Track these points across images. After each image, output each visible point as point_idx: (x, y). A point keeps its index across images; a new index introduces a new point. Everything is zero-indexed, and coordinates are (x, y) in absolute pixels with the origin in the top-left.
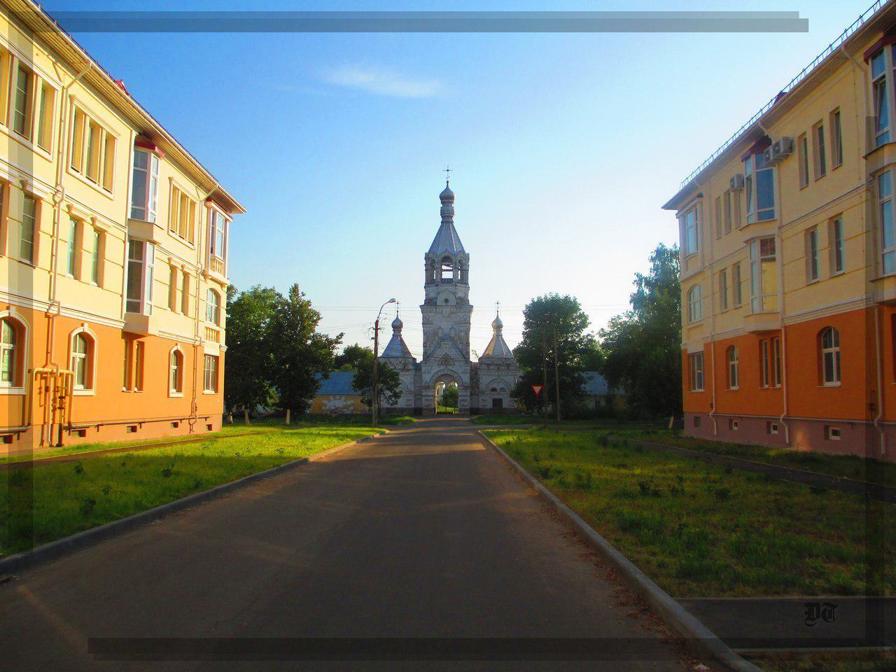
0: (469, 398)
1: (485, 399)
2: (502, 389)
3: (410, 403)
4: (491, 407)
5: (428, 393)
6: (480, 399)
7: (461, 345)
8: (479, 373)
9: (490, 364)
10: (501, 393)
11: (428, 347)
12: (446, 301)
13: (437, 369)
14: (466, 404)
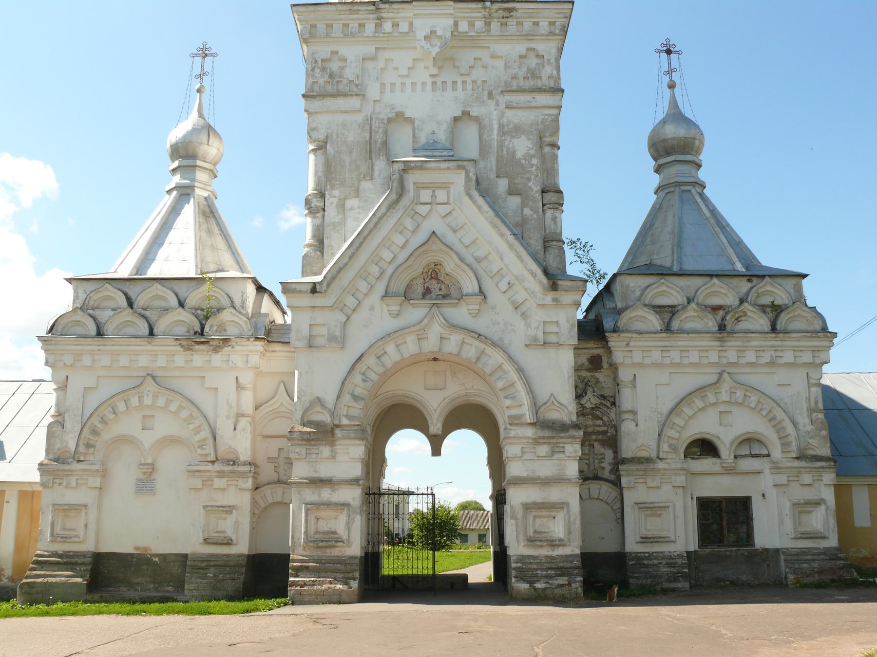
0: (571, 495)
1: (653, 497)
3: (227, 526)
4: (693, 545)
5: (325, 470)
7: (515, 201)
8: (619, 356)
9: (673, 310)
11: (331, 212)
13: (390, 324)
14: (557, 528)
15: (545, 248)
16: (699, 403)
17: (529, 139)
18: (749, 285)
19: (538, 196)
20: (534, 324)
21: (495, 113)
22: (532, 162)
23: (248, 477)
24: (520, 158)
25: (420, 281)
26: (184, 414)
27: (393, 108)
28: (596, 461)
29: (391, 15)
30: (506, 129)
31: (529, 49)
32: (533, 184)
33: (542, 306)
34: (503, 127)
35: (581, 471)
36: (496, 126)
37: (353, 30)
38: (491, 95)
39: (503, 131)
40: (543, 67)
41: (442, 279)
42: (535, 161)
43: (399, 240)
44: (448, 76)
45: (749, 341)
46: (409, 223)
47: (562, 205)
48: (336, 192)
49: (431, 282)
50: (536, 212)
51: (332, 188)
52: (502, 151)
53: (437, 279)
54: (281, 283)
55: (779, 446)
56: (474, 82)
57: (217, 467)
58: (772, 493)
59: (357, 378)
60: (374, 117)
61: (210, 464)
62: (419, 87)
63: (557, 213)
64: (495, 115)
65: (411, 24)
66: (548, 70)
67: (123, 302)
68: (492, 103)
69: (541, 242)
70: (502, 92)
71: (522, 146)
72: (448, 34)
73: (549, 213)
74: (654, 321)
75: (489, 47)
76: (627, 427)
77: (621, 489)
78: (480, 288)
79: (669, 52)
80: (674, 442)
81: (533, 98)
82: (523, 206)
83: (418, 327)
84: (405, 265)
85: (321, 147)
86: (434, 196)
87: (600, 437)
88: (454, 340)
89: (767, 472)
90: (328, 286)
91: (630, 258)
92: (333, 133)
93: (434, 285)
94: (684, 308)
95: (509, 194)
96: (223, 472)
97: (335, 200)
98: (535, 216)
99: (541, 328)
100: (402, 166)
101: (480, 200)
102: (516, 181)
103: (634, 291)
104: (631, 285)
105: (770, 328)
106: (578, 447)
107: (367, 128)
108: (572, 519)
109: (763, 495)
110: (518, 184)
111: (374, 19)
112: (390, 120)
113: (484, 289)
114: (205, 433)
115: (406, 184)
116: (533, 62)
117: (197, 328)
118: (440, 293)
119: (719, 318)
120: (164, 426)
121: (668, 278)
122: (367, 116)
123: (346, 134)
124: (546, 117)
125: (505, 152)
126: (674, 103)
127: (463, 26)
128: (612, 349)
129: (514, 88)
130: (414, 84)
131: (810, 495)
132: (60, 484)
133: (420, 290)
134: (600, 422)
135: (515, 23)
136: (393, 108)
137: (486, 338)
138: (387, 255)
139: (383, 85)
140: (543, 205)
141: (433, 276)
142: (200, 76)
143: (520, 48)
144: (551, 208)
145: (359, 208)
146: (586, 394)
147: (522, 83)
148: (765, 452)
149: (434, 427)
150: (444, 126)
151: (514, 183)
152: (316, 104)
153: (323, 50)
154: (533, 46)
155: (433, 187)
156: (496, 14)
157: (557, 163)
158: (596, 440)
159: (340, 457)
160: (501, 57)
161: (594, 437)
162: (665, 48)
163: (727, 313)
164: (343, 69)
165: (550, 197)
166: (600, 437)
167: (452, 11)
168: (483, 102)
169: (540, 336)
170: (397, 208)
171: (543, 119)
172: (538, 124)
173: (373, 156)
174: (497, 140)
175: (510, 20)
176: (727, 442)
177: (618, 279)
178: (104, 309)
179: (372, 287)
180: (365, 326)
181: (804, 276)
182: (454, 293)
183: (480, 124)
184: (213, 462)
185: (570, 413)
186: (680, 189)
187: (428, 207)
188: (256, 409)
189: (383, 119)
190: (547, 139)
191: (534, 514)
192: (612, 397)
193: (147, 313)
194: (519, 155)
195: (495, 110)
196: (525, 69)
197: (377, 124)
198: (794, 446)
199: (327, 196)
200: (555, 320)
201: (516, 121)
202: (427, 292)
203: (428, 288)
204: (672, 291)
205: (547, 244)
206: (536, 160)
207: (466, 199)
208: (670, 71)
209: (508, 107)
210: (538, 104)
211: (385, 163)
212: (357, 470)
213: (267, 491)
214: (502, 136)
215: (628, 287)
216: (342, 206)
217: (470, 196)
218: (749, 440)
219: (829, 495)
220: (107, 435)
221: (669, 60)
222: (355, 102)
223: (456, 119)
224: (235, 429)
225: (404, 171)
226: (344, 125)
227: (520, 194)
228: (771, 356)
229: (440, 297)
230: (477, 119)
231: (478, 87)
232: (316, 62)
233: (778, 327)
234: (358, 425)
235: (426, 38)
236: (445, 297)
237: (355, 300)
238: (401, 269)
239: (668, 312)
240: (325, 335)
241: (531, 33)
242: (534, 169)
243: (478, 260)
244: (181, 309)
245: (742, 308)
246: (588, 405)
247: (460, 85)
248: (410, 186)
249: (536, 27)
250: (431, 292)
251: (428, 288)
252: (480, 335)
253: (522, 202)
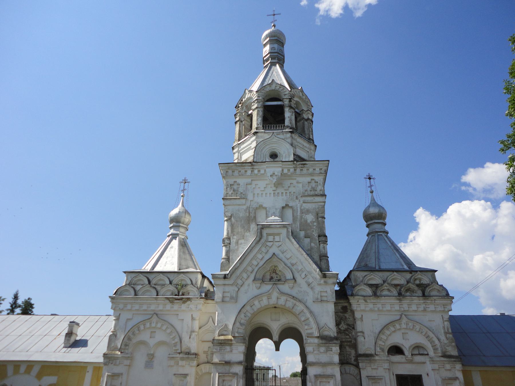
0: (336, 371)
1: (374, 373)
2: (418, 349)
5: (228, 358)
6: (364, 374)
7: (307, 240)
8: (354, 306)
10: (418, 358)
11: (233, 245)
13: (257, 292)
15: (320, 260)
16: (392, 329)
17: (313, 215)
18: (411, 275)
19: (317, 238)
20: (316, 292)
21: (299, 204)
22: (314, 224)
23: (194, 360)
24: (309, 223)
25: (268, 274)
26: (169, 331)
27: (258, 203)
28: (348, 355)
29: (257, 167)
30: (303, 211)
31: (312, 180)
32: (315, 233)
33: (320, 284)
34: (302, 210)
35: (340, 360)
36: (299, 210)
37: (243, 173)
38: (297, 198)
39: (302, 212)
40: (318, 186)
41: (278, 273)
42: (315, 224)
43: (260, 256)
44: (280, 190)
45: (413, 300)
46: (263, 249)
47: (327, 242)
48: (235, 237)
49: (273, 274)
50: (316, 245)
51: (234, 235)
52: (302, 220)
53: (276, 273)
54: (212, 274)
55: (432, 350)
56: (290, 193)
57: (181, 355)
58: (431, 373)
59: (242, 315)
60: (250, 207)
61: (178, 355)
62: (268, 195)
63: (325, 245)
64: (299, 205)
65: (265, 171)
66: (320, 188)
67: (147, 282)
68: (297, 201)
69: (319, 257)
70: (301, 196)
71: (310, 218)
72: (280, 174)
73: (322, 245)
74: (369, 291)
75: (296, 179)
76: (360, 339)
77: (360, 369)
78: (293, 277)
79: (370, 178)
80: (383, 347)
81: (314, 199)
82: (311, 242)
83: (268, 293)
84: (263, 267)
85: (229, 220)
86: (274, 239)
87: (348, 344)
88: (283, 299)
89: (428, 363)
90: (231, 275)
91: (357, 264)
92: (234, 213)
93: (274, 275)
94: (382, 285)
95: (305, 237)
96: (183, 358)
97: (235, 240)
98: (316, 246)
99: (320, 294)
100: (261, 226)
101: (293, 240)
102: (308, 232)
103: (360, 278)
104: (358, 275)
105: (422, 294)
106: (338, 348)
107: (248, 211)
108: (337, 383)
109: (428, 374)
110: (309, 233)
111: (251, 169)
112: (257, 208)
113: (295, 277)
114: (177, 340)
115: (263, 233)
116: (313, 184)
117: (177, 293)
118: (277, 279)
119: (398, 290)
120: (160, 336)
121: (374, 272)
122: (248, 206)
123: (239, 213)
124: (319, 206)
125: (303, 220)
126: (373, 199)
127: (285, 171)
128: (351, 303)
129: (306, 195)
130: (266, 194)
131: (449, 375)
132: (112, 363)
133: (268, 277)
134: (348, 337)
135: (306, 169)
136: (258, 203)
137: (296, 298)
138: (255, 263)
139: (254, 194)
140: (319, 242)
141: (274, 271)
142: (183, 191)
143: (308, 179)
144: (322, 243)
145: (244, 243)
146: (341, 324)
147: (309, 193)
148: (426, 353)
149: (275, 338)
150: (278, 210)
151: (307, 233)
152: (228, 202)
153: (231, 181)
154: (313, 178)
155: (274, 235)
156: (298, 166)
157: (324, 224)
158: (347, 345)
159: (234, 351)
160: (300, 183)
161: (346, 344)
162: (368, 177)
163: (402, 287)
164: (238, 188)
165: (323, 239)
166: (348, 344)
167: (281, 165)
168: (294, 200)
169: (319, 297)
170: (259, 243)
171: (318, 207)
172: (316, 209)
173: (250, 222)
174: (300, 216)
175: (304, 168)
176: (407, 347)
177: (352, 273)
178: (138, 285)
179: (248, 277)
180: (246, 293)
181: (436, 271)
182: (283, 279)
183: (293, 209)
184: (179, 353)
185: (334, 332)
186: (377, 234)
187: (272, 243)
188: (200, 328)
189: (254, 208)
190: (320, 215)
191: (320, 380)
192: (353, 325)
193: (156, 286)
194: (309, 221)
195: (299, 203)
196: (310, 187)
197: (252, 210)
198: (439, 350)
199: (231, 239)
200: (325, 290)
201: (307, 208)
202: (271, 278)
203: (272, 276)
204: (376, 278)
205: (321, 258)
206: (316, 224)
207: (287, 240)
208: (371, 186)
209: (304, 202)
210: (316, 201)
211: (255, 225)
212: (241, 357)
213: (202, 366)
214: (301, 214)
215: (357, 276)
216: (237, 243)
217: (289, 239)
218: (418, 347)
219: (460, 375)
220: (134, 341)
221: (370, 181)
222: (243, 201)
223: (283, 208)
224: (190, 338)
225: (262, 228)
226: (239, 210)
227: (310, 237)
228: (424, 307)
229: (277, 280)
230: (291, 207)
231: (292, 195)
232: (228, 185)
233: (426, 294)
234: (242, 337)
235: (271, 176)
236: (279, 280)
237: (242, 282)
238: (261, 269)
239: (375, 287)
240: (229, 297)
241: (312, 173)
242: (315, 227)
243: (293, 265)
244: (170, 285)
245: (408, 285)
246: (342, 329)
247: (284, 194)
248: (264, 234)
249: (314, 171)
250: (273, 279)
251: (272, 276)
252: (293, 297)
253: (311, 241)
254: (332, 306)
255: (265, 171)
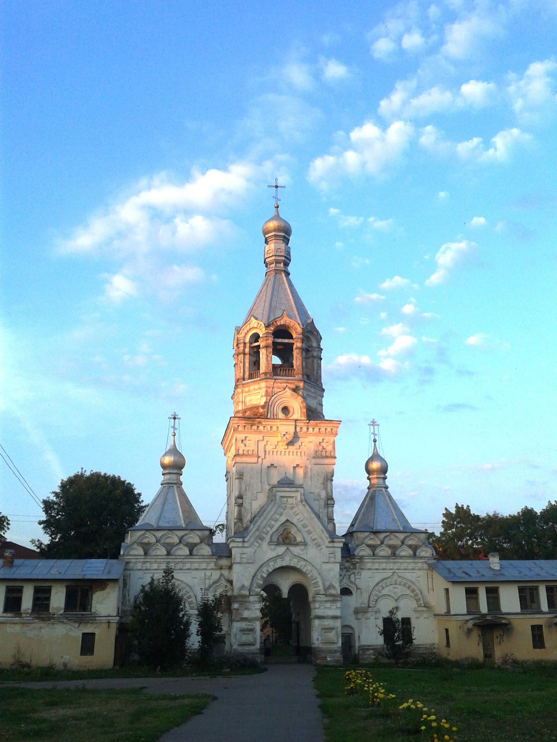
12: (285, 410)
65: (278, 427)
88: (295, 560)
165: (329, 502)
191: (324, 631)
254: (337, 567)
255: (278, 427)
